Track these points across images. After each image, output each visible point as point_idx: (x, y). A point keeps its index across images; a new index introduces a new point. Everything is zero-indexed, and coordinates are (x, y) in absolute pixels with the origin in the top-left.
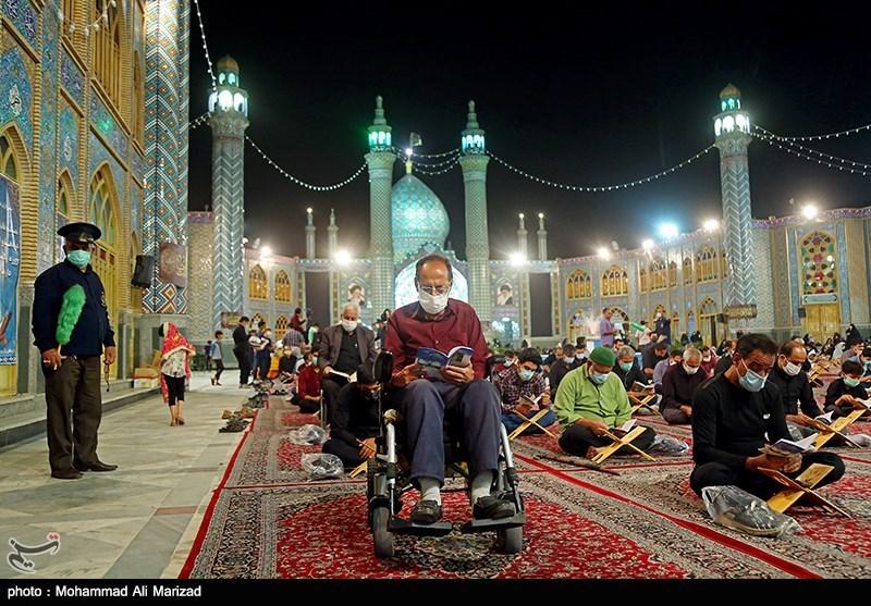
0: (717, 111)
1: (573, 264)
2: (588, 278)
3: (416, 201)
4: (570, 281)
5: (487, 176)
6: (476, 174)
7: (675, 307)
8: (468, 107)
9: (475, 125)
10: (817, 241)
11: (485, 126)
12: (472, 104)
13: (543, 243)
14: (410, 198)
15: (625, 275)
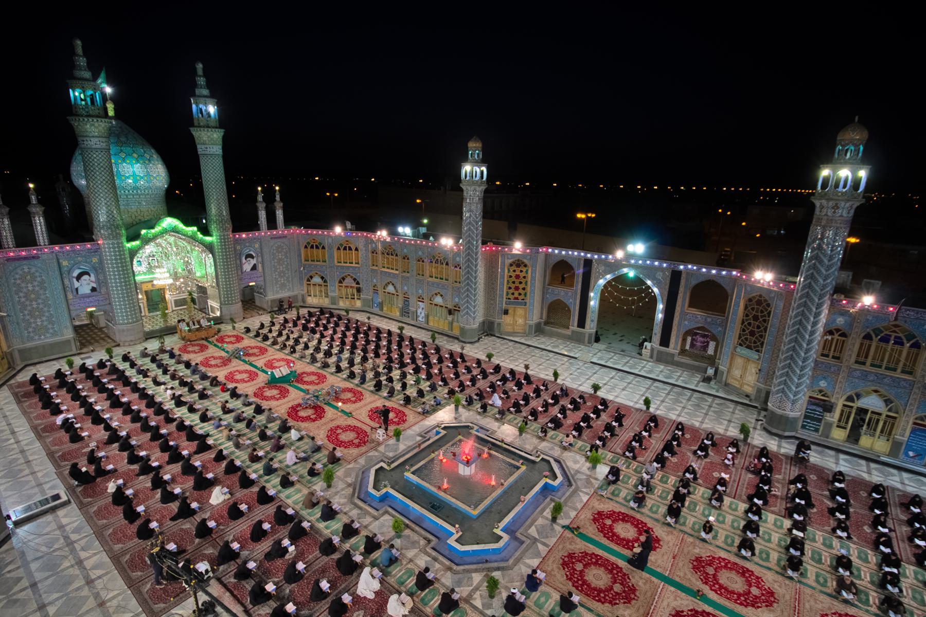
0: (465, 159)
1: (308, 234)
2: (323, 248)
3: (128, 155)
4: (306, 247)
5: (224, 148)
6: (210, 144)
7: (406, 288)
8: (195, 69)
9: (205, 92)
10: (518, 266)
11: (216, 95)
12: (200, 66)
13: (280, 214)
14: (121, 151)
15: (356, 249)
